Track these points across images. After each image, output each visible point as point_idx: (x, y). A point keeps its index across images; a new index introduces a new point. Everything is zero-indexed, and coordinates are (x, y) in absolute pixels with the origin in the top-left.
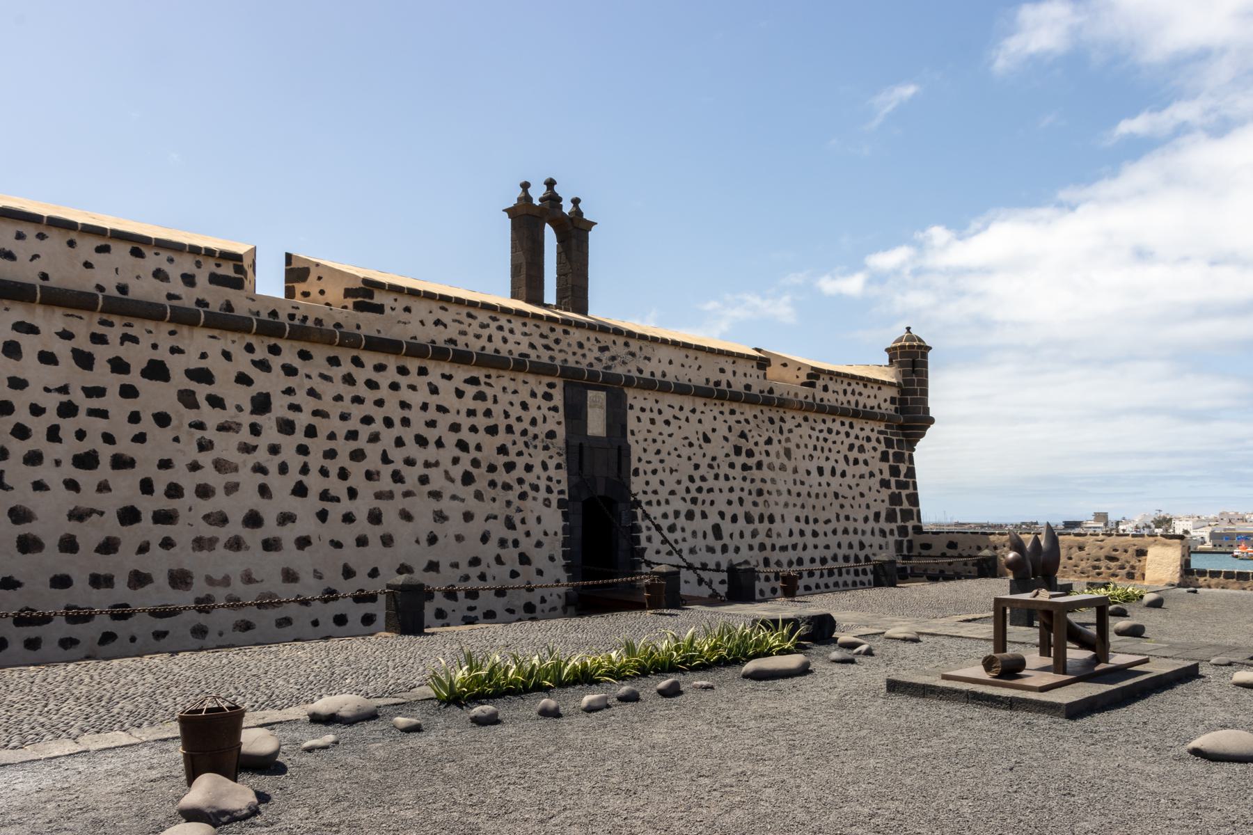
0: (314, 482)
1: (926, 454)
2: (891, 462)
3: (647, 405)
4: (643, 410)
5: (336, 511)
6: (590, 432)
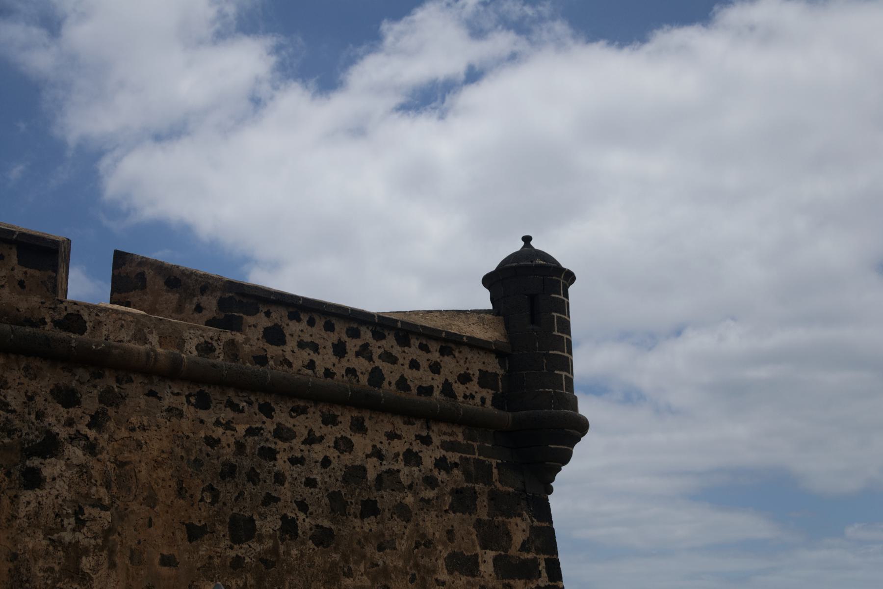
2: (483, 514)
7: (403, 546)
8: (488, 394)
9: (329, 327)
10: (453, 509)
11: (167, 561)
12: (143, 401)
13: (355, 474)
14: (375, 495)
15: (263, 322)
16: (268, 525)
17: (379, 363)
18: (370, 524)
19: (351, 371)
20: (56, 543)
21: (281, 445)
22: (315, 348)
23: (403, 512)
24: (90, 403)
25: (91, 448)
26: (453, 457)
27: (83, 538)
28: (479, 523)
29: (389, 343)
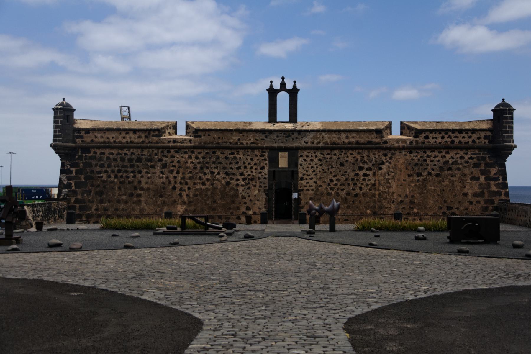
0: (178, 186)
1: (510, 163)
3: (310, 155)
4: (307, 156)
5: (184, 194)
6: (280, 166)
7: (458, 176)
8: (487, 141)
9: (440, 133)
10: (473, 167)
11: (404, 180)
12: (399, 154)
13: (447, 162)
14: (451, 166)
15: (423, 135)
16: (425, 173)
17: (453, 139)
18: (450, 172)
19: (446, 142)
20: (385, 178)
21: (428, 158)
22: (436, 138)
23: (459, 169)
24: (389, 155)
25: (390, 163)
26: (473, 156)
27: (389, 177)
28: (481, 170)
29: (457, 134)
